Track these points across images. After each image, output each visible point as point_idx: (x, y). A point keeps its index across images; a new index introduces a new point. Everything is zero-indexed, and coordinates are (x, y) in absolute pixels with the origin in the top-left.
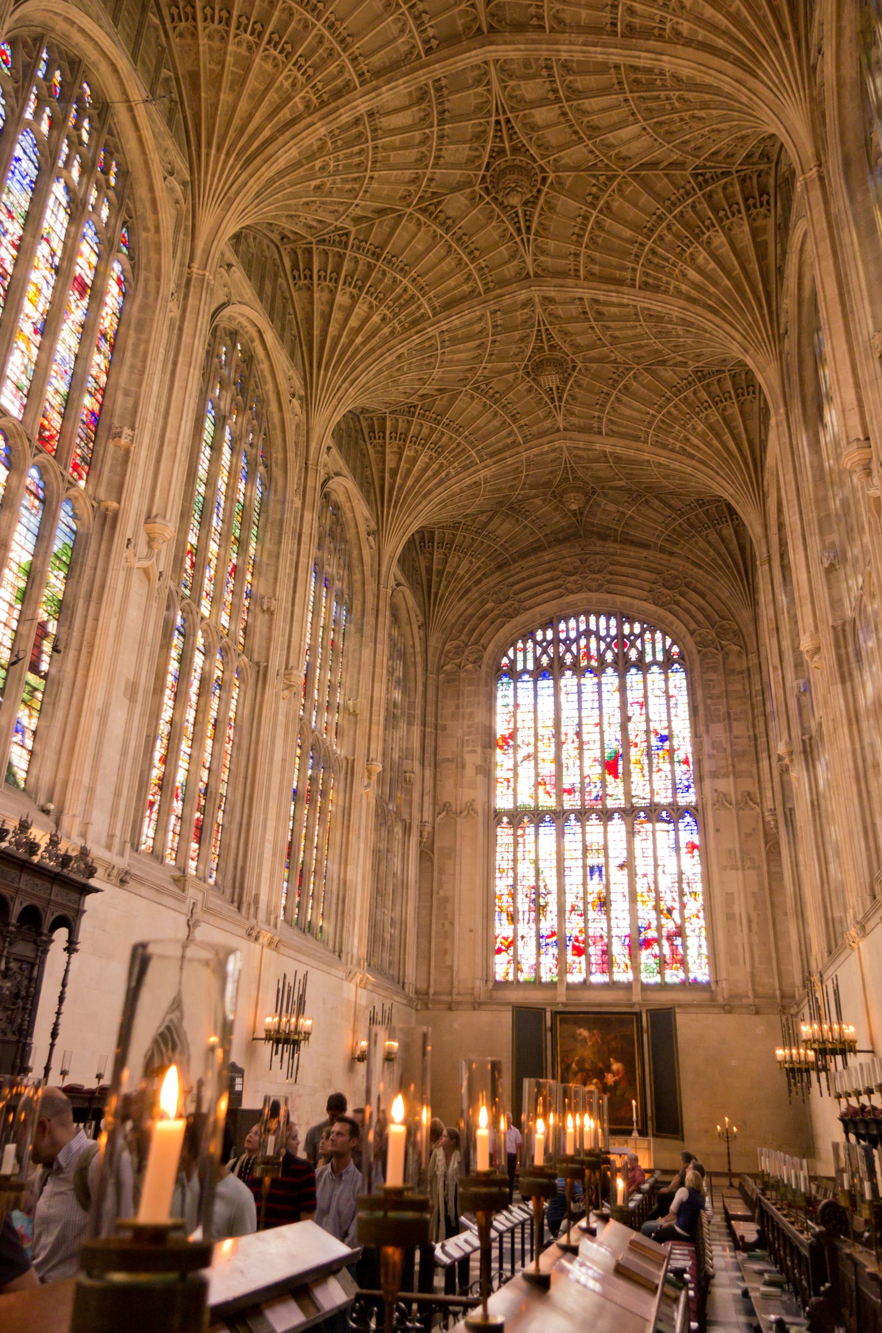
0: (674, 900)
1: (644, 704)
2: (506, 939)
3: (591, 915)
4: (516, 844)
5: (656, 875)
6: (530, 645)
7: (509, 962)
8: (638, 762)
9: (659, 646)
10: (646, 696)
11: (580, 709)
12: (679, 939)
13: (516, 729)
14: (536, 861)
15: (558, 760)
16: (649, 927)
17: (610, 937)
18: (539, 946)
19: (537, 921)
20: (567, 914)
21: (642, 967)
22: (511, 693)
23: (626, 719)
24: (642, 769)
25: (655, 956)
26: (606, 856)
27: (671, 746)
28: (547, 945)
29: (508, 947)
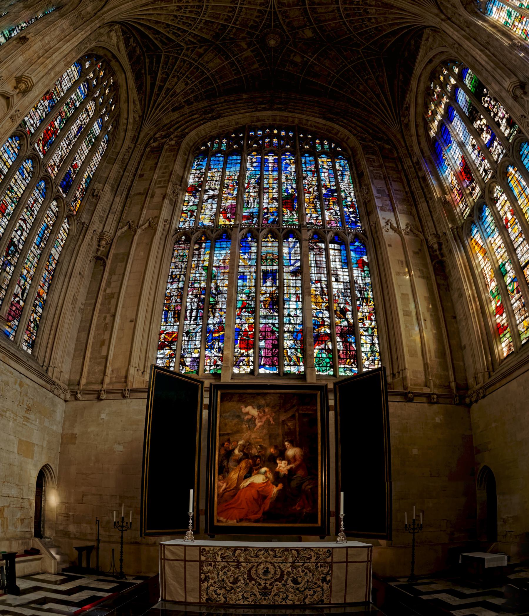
0: (346, 303)
1: (317, 171)
6: (225, 141)
13: (205, 181)
14: (208, 269)
15: (239, 197)
16: (323, 325)
18: (205, 340)
19: (204, 318)
21: (316, 360)
22: (204, 163)
23: (299, 178)
24: (315, 207)
25: (328, 351)
27: (339, 195)
28: (215, 338)
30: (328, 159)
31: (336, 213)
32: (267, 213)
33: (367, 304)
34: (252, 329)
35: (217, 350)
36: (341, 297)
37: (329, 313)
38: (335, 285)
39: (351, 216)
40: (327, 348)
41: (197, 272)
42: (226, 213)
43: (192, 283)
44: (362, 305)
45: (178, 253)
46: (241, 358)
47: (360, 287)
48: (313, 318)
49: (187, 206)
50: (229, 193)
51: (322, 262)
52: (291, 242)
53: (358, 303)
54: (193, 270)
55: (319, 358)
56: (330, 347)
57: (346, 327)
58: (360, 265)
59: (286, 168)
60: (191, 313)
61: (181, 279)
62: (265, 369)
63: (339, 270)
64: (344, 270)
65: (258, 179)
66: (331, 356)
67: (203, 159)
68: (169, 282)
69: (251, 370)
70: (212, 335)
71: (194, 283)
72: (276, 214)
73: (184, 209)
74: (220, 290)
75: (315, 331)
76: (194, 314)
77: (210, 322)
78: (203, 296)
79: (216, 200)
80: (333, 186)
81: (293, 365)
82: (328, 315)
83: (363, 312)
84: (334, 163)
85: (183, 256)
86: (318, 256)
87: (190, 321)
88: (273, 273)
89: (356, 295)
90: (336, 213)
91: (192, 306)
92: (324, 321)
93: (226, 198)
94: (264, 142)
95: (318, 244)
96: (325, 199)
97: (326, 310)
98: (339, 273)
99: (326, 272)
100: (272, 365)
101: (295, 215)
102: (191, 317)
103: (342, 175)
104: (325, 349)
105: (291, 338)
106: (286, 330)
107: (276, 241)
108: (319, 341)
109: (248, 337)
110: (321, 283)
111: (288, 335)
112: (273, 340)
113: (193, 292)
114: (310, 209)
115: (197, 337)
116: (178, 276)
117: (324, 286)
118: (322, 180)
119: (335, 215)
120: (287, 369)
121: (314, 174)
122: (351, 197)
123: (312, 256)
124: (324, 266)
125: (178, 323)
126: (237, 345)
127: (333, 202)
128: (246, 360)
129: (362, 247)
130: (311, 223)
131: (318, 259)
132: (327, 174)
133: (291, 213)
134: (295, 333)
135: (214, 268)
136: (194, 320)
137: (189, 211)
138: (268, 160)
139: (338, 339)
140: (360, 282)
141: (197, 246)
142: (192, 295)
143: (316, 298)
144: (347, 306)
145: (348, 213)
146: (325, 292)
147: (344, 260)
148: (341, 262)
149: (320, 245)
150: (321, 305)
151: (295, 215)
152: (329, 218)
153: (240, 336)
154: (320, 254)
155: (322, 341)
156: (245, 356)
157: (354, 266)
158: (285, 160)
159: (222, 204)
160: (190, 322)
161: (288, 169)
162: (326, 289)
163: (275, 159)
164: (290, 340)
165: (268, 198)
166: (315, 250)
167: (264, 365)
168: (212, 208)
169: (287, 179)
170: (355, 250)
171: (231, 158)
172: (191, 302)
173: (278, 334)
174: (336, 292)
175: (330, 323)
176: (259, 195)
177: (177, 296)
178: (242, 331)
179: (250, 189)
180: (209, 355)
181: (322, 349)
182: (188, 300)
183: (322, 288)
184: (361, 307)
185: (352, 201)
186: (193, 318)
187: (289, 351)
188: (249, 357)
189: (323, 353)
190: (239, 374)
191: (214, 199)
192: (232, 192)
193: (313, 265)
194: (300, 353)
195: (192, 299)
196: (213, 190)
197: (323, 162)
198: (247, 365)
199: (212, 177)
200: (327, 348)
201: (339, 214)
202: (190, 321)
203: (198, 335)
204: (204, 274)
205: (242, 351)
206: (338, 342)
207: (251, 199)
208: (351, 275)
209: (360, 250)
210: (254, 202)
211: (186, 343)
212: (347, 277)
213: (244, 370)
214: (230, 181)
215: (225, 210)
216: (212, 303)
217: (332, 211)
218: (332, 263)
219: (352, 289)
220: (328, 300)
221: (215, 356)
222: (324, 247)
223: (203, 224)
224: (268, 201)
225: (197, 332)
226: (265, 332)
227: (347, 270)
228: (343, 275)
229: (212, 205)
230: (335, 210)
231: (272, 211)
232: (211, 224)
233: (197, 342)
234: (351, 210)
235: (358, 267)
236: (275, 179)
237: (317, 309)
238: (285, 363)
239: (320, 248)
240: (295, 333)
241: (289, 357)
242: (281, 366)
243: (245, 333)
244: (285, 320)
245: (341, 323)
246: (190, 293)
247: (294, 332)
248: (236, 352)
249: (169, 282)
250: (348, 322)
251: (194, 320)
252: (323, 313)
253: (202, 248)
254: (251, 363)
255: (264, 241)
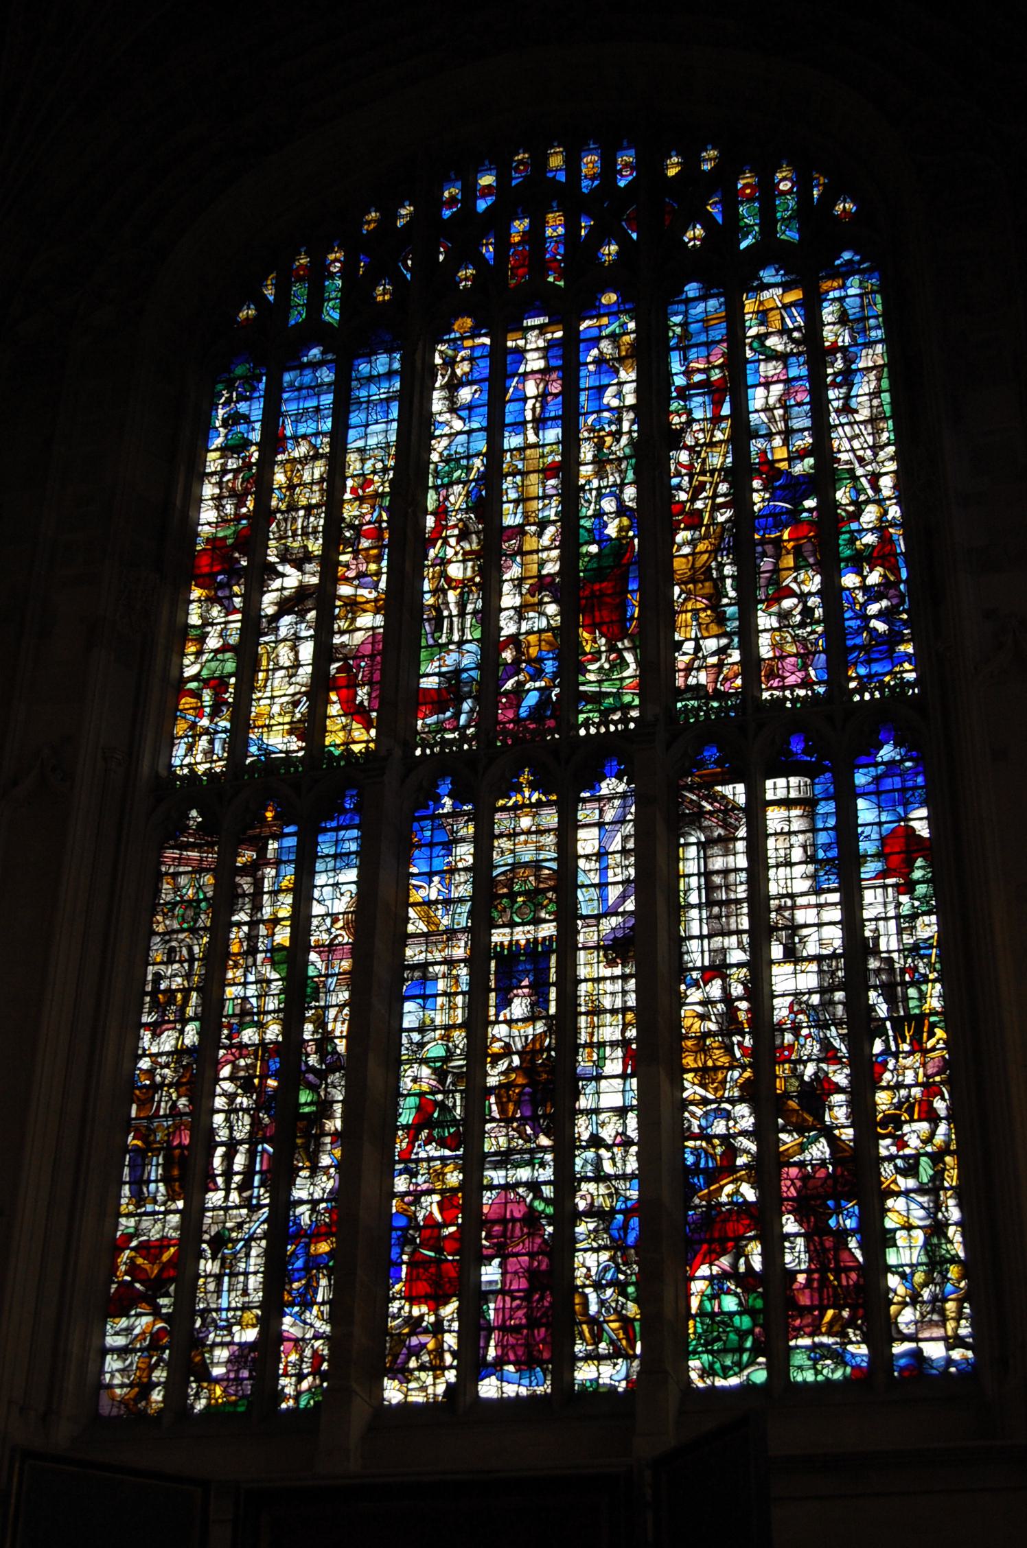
0: (829, 1054)
2: (150, 1250)
3: (496, 1139)
4: (226, 900)
5: (759, 967)
7: (155, 1343)
8: (701, 576)
9: (786, 206)
10: (736, 366)
11: (495, 430)
12: (852, 1206)
13: (264, 514)
16: (727, 1168)
17: (567, 1216)
20: (401, 1145)
25: (747, 1281)
26: (568, 917)
27: (828, 505)
29: (157, 1287)
30: (787, 287)
31: (807, 612)
32: (514, 668)
33: (918, 1047)
34: (452, 1212)
35: (326, 1308)
36: (805, 1032)
37: (755, 1111)
38: (784, 979)
39: (873, 609)
40: (742, 1269)
41: (251, 978)
42: (353, 685)
43: (230, 1026)
44: (896, 1055)
45: (177, 889)
46: (414, 1341)
47: (891, 970)
48: (690, 1144)
49: (199, 653)
50: (361, 575)
51: (732, 877)
52: (610, 799)
53: (878, 1046)
54: (236, 966)
55: (712, 1315)
56: (757, 1263)
57: (823, 1163)
58: (896, 860)
59: (601, 389)
60: (229, 1158)
61: (190, 1012)
62: (501, 1380)
63: (801, 901)
64: (822, 899)
65: (482, 477)
66: (759, 1304)
67: (251, 381)
68: (147, 1026)
69: (449, 1385)
70: (307, 1246)
71: (242, 1026)
72: (549, 667)
73: (189, 672)
74: (335, 1052)
75: (697, 1201)
76: (240, 1162)
77: (298, 1194)
78: (272, 1083)
79: (312, 615)
80: (801, 455)
81: (608, 1357)
82: (747, 1123)
83: (899, 1086)
84: (811, 307)
85: (193, 904)
86: (716, 850)
87: (228, 1190)
88: (535, 953)
89: (872, 1008)
90: (807, 612)
91: (231, 1129)
92: (733, 1152)
93: (354, 606)
94: (503, 244)
95: (719, 788)
96: (763, 542)
97: (741, 1100)
98: (801, 917)
99: (745, 923)
100: (526, 1365)
101: (629, 657)
102: (228, 1173)
103: (847, 378)
104: (731, 1275)
105: (605, 1240)
106: (582, 1205)
107: (549, 804)
108: (710, 1241)
109: (439, 1251)
110: (724, 977)
111: (591, 1226)
112: (531, 1255)
113: (236, 1068)
114: (696, 612)
115: (252, 1261)
116: (179, 996)
117: (737, 990)
118: (757, 436)
119: (802, 625)
120: (585, 1373)
121: (718, 405)
122: (879, 502)
123: (692, 852)
124: (741, 892)
125: (180, 1204)
126: (398, 1287)
127: (798, 552)
128: (431, 1346)
129: (908, 764)
130: (698, 685)
131: (718, 863)
132: (777, 389)
133: (612, 648)
134: (620, 1217)
135: (313, 956)
136: (241, 1189)
137: (206, 683)
138: (520, 353)
139: (790, 1225)
140: (889, 943)
141: (247, 856)
142: (231, 1078)
143: (702, 1049)
144: (833, 1068)
145: (860, 597)
146: (742, 1016)
147: (827, 847)
148: (810, 859)
149: (727, 790)
150: (724, 1081)
151: (629, 657)
152: (774, 646)
153: (407, 1249)
154: (726, 842)
155: (723, 1240)
156: (426, 1331)
157: (870, 869)
158: (595, 341)
159: (337, 640)
160: (226, 1198)
161: (609, 398)
162: (743, 1005)
163: (551, 344)
164: (596, 1250)
165: (519, 583)
166: (706, 823)
167: (500, 1362)
168: (297, 665)
169: (600, 462)
170: (876, 792)
171: (364, 368)
172: (230, 1111)
173: (550, 1229)
174: (785, 1012)
175: (758, 1157)
176: (481, 571)
177: (176, 1085)
178: (417, 1227)
179: (446, 543)
180: (296, 1332)
181: (724, 1275)
182: (220, 1102)
183: (727, 999)
184: (891, 1064)
185: (881, 528)
186: (237, 1178)
187: (593, 1297)
188: (443, 1332)
189: (729, 1292)
190: (405, 1406)
191: (301, 615)
192: (373, 567)
193: (694, 898)
194: (635, 1301)
195: (231, 1097)
196: (299, 565)
197: (763, 316)
198: (433, 1368)
199: (291, 487)
200: (742, 1269)
201: (818, 613)
202: (228, 1190)
203: (254, 1253)
204: (276, 986)
205: (416, 1312)
206: (787, 1237)
207: (452, 596)
208: (852, 921)
209: (896, 782)
210: (462, 614)
211: (211, 1287)
212: (834, 935)
213: (423, 1388)
214: (366, 508)
215: (345, 668)
216: (307, 1110)
217: (787, 603)
218: (772, 873)
219: (856, 983)
220: (753, 1052)
221: (316, 1337)
222: (741, 800)
223: (266, 751)
224: (517, 601)
225: (252, 1238)
226: (503, 1221)
227: (835, 897)
228: (820, 925)
229: (294, 649)
230: (803, 597)
231: (533, 652)
232: (295, 744)
233: (254, 1282)
234: (874, 578)
235: (882, 875)
236: (548, 472)
237: (705, 1101)
238: (579, 1348)
239: (728, 808)
240: (620, 1217)
241: (593, 1321)
242: (565, 1363)
243: (428, 1232)
244: (582, 1161)
245: (802, 1148)
246: (226, 1072)
247: (613, 1211)
248: (394, 1317)
249: (147, 1026)
250: (834, 1142)
251: (241, 1189)
252: (728, 1116)
253: (267, 863)
254: (448, 1359)
255: (504, 809)
